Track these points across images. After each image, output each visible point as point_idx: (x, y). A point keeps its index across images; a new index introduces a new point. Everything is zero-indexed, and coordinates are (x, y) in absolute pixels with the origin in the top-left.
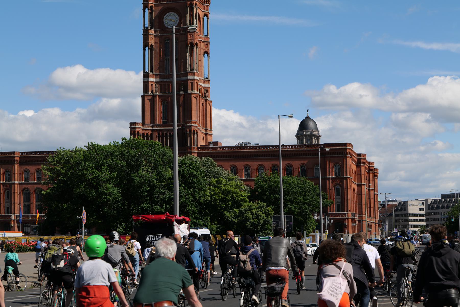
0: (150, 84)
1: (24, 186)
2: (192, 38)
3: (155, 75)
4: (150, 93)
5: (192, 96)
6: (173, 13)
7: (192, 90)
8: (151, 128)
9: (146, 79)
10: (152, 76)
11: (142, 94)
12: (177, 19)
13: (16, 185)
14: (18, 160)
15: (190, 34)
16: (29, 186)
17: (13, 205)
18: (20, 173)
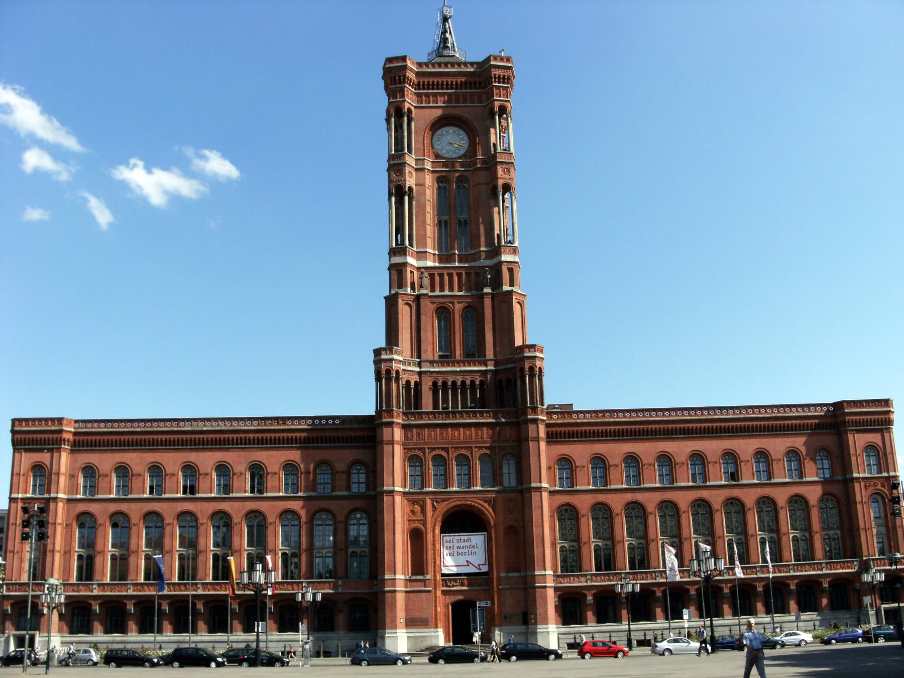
0: (409, 269)
1: (82, 507)
2: (507, 176)
3: (417, 252)
4: (409, 289)
5: (514, 297)
6: (454, 129)
7: (512, 284)
8: (417, 369)
9: (397, 260)
10: (412, 254)
11: (387, 294)
12: (464, 140)
13: (60, 505)
14: (68, 440)
15: (504, 166)
16: (93, 508)
17: (49, 556)
18: (72, 473)
